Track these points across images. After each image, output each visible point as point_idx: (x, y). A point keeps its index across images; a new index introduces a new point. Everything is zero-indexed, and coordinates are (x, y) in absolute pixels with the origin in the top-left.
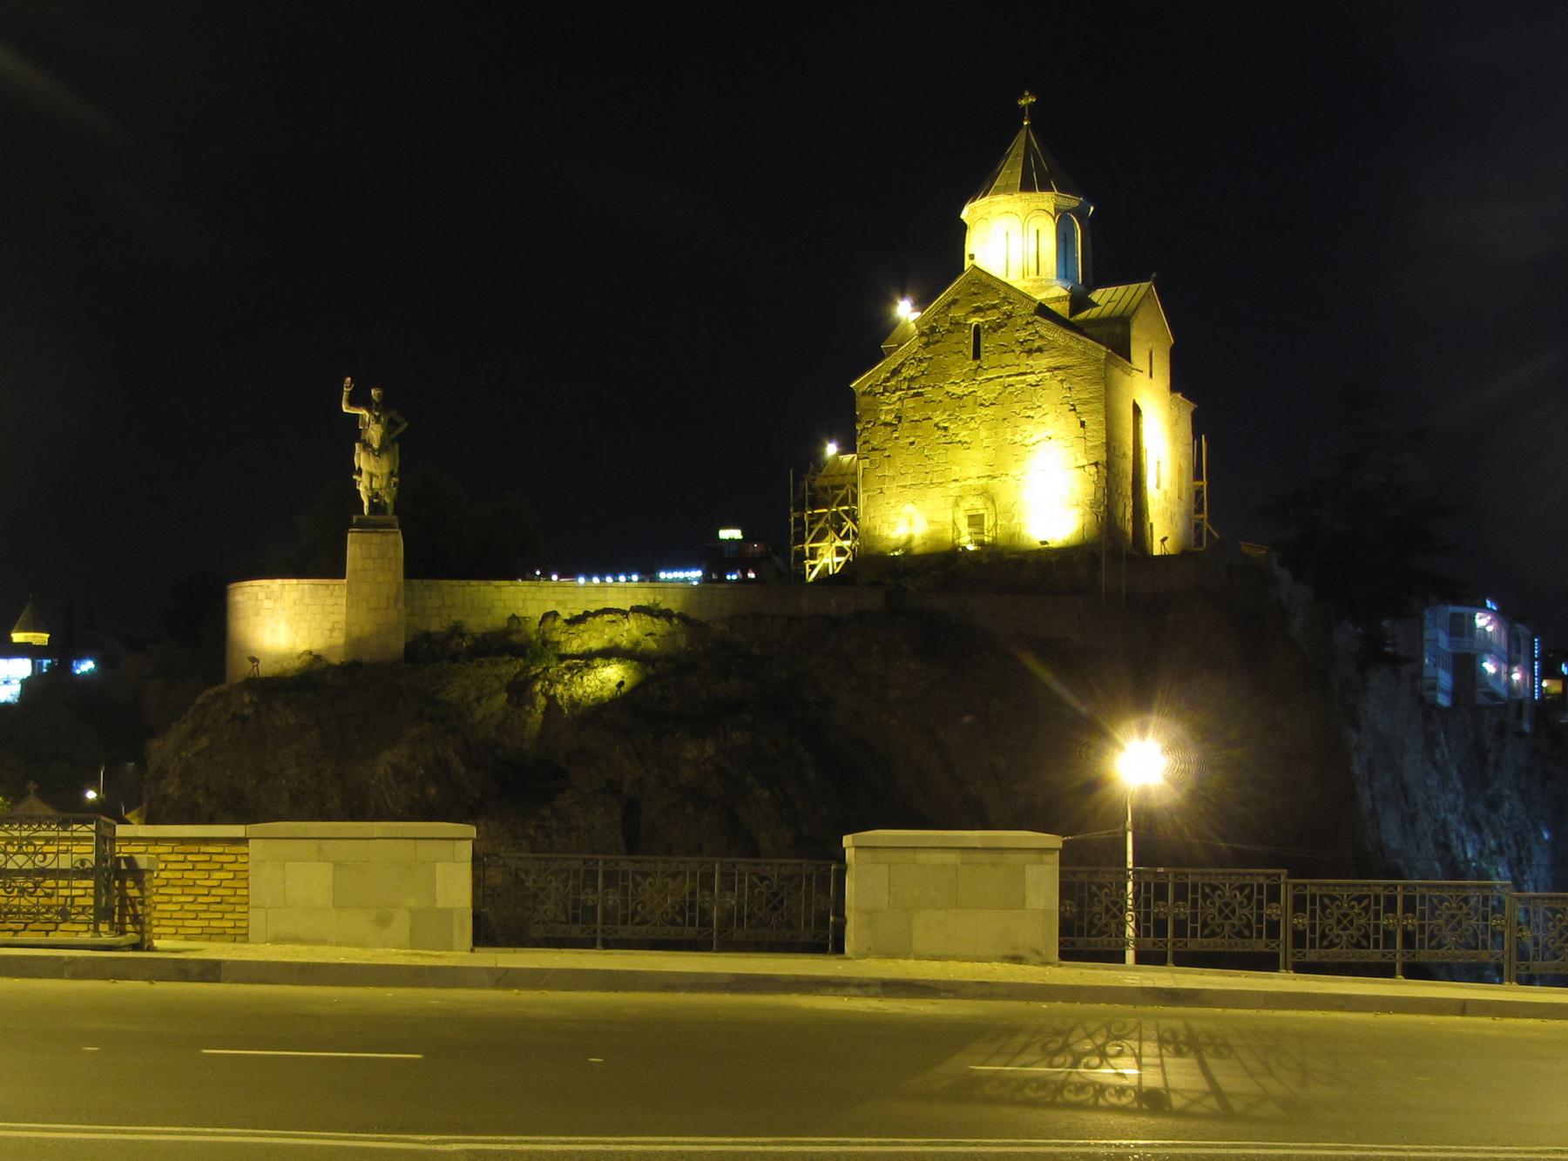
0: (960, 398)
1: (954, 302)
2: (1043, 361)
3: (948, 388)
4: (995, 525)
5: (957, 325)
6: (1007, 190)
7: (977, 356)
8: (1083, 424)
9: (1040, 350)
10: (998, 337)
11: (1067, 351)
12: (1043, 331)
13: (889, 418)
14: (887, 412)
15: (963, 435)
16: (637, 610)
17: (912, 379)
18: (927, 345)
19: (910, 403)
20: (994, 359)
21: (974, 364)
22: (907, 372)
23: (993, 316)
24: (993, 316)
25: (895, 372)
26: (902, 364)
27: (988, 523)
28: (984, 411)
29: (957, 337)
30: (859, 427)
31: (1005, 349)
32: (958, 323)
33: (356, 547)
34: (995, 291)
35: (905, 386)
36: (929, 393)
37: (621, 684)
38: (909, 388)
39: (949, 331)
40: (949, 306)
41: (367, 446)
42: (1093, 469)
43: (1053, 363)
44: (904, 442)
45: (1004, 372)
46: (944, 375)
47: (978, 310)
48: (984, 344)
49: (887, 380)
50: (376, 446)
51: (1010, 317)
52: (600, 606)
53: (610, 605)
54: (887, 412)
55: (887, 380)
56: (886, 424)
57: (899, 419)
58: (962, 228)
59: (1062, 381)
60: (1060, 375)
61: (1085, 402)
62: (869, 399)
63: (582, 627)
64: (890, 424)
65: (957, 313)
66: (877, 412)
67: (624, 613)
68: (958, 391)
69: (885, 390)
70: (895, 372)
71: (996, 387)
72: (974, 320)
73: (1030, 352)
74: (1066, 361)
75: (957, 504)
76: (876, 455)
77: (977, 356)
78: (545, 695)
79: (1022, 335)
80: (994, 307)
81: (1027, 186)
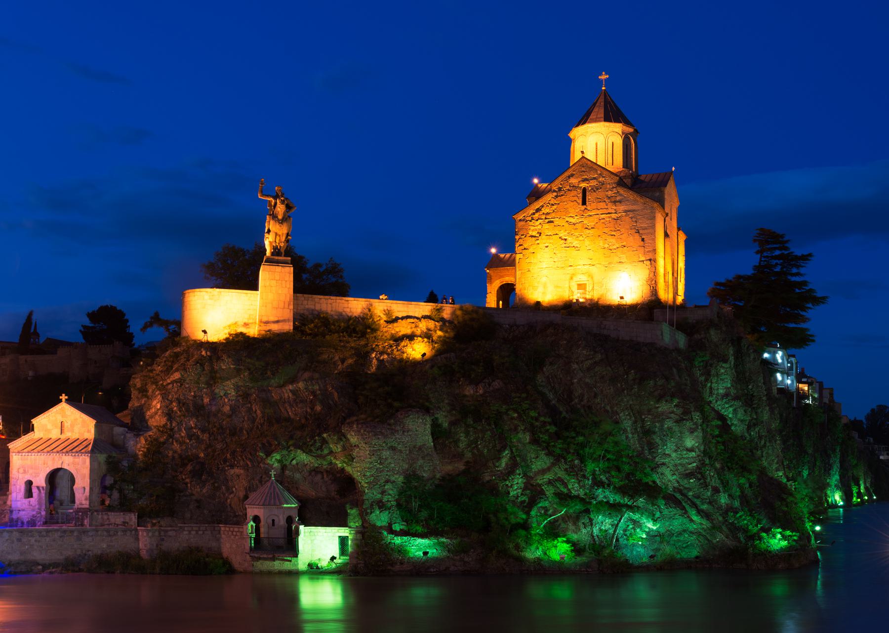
0: (574, 224)
1: (572, 175)
2: (622, 208)
3: (567, 219)
4: (593, 289)
5: (575, 187)
6: (596, 121)
7: (584, 203)
8: (643, 240)
9: (620, 202)
11: (635, 202)
13: (534, 234)
15: (575, 243)
16: (425, 317)
17: (548, 214)
18: (557, 196)
19: (546, 226)
20: (594, 205)
21: (583, 207)
22: (546, 210)
23: (594, 183)
24: (594, 183)
25: (538, 210)
26: (542, 206)
27: (589, 288)
28: (588, 231)
29: (574, 193)
30: (517, 237)
31: (599, 200)
33: (265, 274)
35: (543, 217)
36: (557, 221)
37: (424, 355)
40: (569, 177)
41: (274, 217)
43: (626, 208)
44: (542, 246)
45: (599, 212)
46: (566, 211)
47: (584, 180)
49: (534, 214)
52: (405, 314)
55: (534, 214)
56: (532, 236)
58: (569, 141)
59: (631, 218)
61: (645, 229)
62: (522, 223)
63: (395, 325)
65: (573, 181)
67: (418, 318)
68: (571, 220)
70: (538, 210)
71: (595, 219)
72: (583, 185)
73: (615, 202)
74: (634, 207)
75: (572, 278)
77: (584, 203)
78: (378, 359)
79: (610, 193)
80: (595, 178)
81: (607, 119)
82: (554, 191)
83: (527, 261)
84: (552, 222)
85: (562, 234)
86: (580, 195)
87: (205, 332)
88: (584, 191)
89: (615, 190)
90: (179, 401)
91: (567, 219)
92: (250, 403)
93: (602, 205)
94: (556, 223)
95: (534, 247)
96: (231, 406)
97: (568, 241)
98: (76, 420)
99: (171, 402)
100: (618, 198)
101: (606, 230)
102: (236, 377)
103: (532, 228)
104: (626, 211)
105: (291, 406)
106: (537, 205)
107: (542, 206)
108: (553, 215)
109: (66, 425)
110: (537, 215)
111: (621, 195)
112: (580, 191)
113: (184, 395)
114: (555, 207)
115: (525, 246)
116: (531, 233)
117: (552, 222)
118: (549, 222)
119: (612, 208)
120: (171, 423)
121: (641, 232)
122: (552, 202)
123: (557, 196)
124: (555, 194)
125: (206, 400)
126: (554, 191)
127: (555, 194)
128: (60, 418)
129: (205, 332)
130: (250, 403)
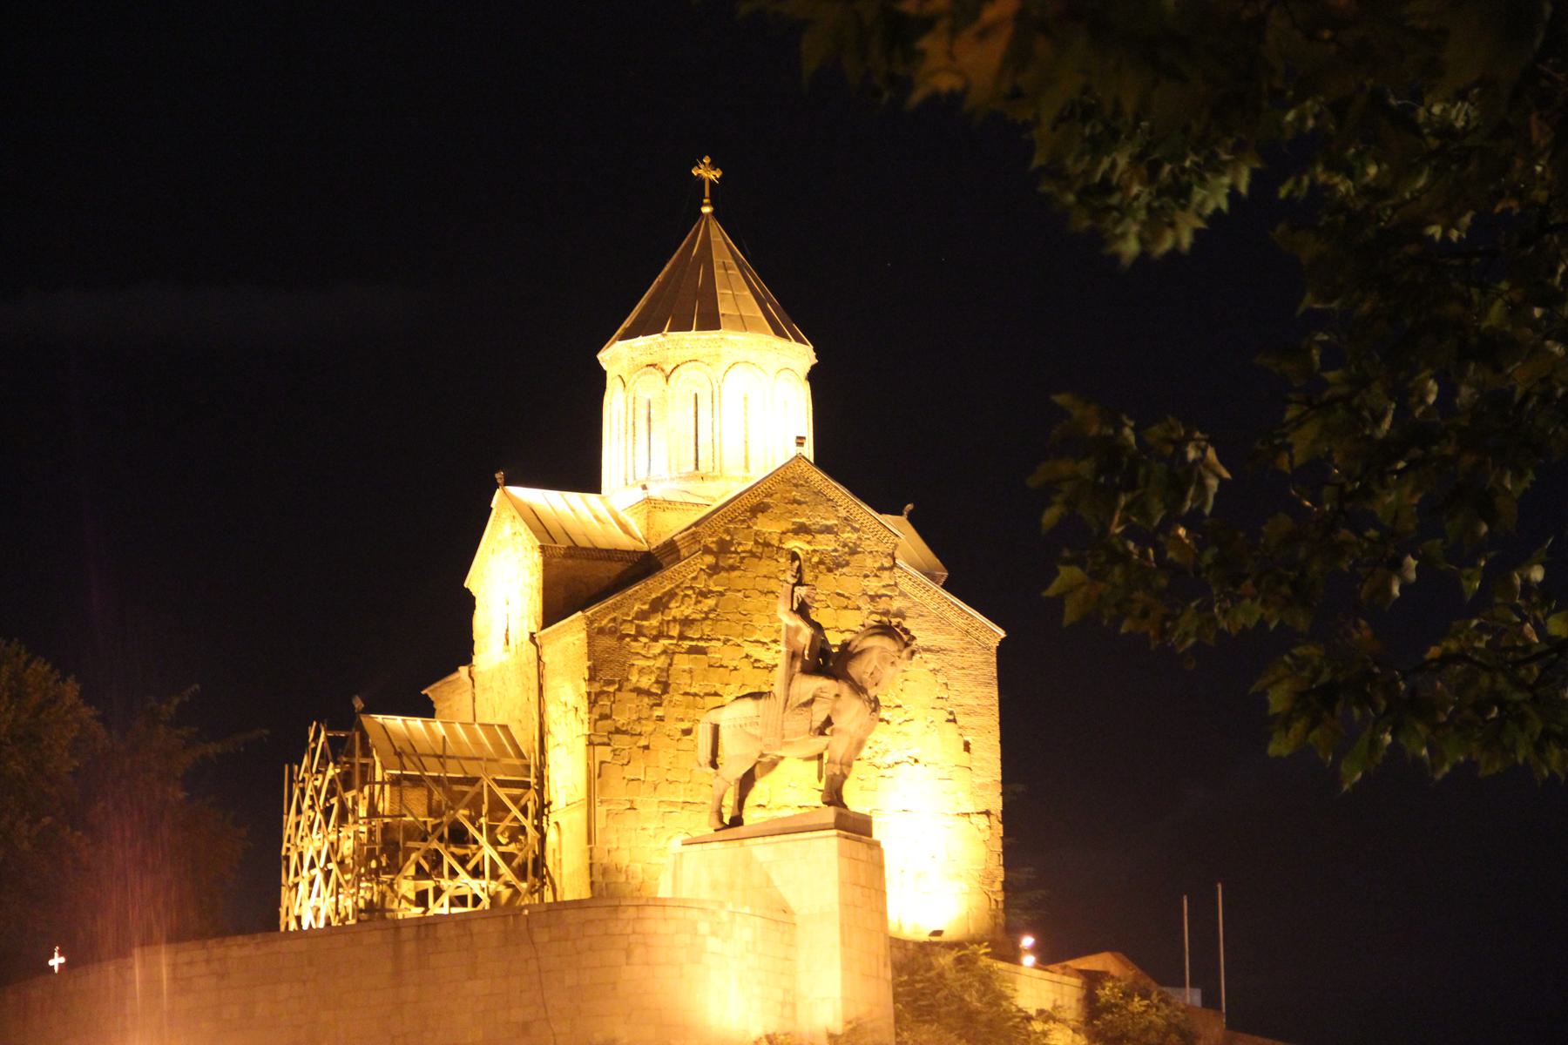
5: (766, 547)
13: (646, 682)
14: (641, 671)
17: (687, 622)
19: (683, 662)
22: (677, 610)
23: (826, 543)
24: (826, 543)
25: (659, 605)
26: (672, 595)
29: (765, 567)
32: (767, 544)
35: (675, 632)
38: (682, 637)
39: (753, 554)
42: (984, 820)
47: (801, 530)
49: (643, 615)
51: (853, 552)
54: (641, 671)
55: (643, 615)
56: (639, 691)
57: (665, 687)
64: (648, 693)
65: (768, 527)
66: (626, 667)
69: (640, 632)
76: (620, 741)
80: (828, 530)
83: (630, 772)
84: (702, 651)
91: (748, 648)
94: (714, 656)
95: (648, 727)
107: (672, 595)
111: (903, 594)
114: (711, 602)
117: (702, 651)
122: (700, 585)
123: (714, 570)
124: (710, 559)
127: (710, 559)
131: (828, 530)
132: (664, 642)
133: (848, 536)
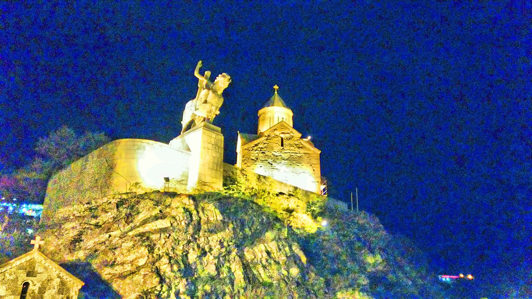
0: (277, 156)
2: (302, 151)
3: (273, 153)
5: (277, 136)
7: (282, 145)
10: (288, 142)
12: (302, 142)
13: (253, 158)
17: (262, 148)
18: (267, 139)
19: (261, 155)
23: (288, 136)
24: (288, 136)
26: (259, 143)
28: (284, 161)
31: (291, 145)
34: (289, 129)
35: (259, 149)
40: (274, 130)
45: (291, 152)
48: (284, 142)
49: (254, 147)
50: (220, 92)
53: (282, 192)
55: (254, 147)
56: (252, 159)
57: (257, 159)
60: (307, 156)
61: (314, 164)
65: (277, 133)
68: (277, 154)
69: (253, 150)
70: (256, 145)
73: (299, 148)
77: (282, 145)
79: (296, 143)
80: (288, 133)
82: (266, 136)
85: (270, 160)
86: (280, 141)
87: (167, 180)
88: (282, 139)
89: (299, 141)
90: (170, 258)
92: (229, 261)
93: (292, 148)
96: (215, 264)
97: (273, 165)
98: (49, 280)
99: (160, 257)
100: (301, 146)
101: (294, 162)
102: (221, 231)
103: (253, 155)
104: (305, 153)
105: (264, 267)
106: (256, 142)
107: (259, 143)
108: (265, 149)
109: (31, 287)
110: (255, 148)
112: (280, 139)
113: (173, 249)
115: (248, 164)
116: (251, 157)
118: (262, 153)
119: (297, 150)
120: (162, 286)
121: (313, 166)
123: (267, 139)
125: (192, 257)
126: (266, 136)
128: (23, 277)
129: (167, 180)
130: (229, 261)
131: (288, 133)
132: (257, 151)
133: (292, 134)
